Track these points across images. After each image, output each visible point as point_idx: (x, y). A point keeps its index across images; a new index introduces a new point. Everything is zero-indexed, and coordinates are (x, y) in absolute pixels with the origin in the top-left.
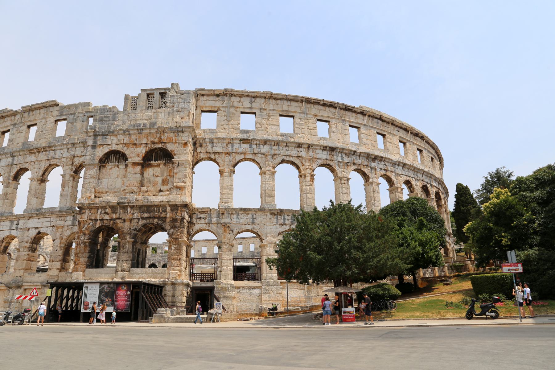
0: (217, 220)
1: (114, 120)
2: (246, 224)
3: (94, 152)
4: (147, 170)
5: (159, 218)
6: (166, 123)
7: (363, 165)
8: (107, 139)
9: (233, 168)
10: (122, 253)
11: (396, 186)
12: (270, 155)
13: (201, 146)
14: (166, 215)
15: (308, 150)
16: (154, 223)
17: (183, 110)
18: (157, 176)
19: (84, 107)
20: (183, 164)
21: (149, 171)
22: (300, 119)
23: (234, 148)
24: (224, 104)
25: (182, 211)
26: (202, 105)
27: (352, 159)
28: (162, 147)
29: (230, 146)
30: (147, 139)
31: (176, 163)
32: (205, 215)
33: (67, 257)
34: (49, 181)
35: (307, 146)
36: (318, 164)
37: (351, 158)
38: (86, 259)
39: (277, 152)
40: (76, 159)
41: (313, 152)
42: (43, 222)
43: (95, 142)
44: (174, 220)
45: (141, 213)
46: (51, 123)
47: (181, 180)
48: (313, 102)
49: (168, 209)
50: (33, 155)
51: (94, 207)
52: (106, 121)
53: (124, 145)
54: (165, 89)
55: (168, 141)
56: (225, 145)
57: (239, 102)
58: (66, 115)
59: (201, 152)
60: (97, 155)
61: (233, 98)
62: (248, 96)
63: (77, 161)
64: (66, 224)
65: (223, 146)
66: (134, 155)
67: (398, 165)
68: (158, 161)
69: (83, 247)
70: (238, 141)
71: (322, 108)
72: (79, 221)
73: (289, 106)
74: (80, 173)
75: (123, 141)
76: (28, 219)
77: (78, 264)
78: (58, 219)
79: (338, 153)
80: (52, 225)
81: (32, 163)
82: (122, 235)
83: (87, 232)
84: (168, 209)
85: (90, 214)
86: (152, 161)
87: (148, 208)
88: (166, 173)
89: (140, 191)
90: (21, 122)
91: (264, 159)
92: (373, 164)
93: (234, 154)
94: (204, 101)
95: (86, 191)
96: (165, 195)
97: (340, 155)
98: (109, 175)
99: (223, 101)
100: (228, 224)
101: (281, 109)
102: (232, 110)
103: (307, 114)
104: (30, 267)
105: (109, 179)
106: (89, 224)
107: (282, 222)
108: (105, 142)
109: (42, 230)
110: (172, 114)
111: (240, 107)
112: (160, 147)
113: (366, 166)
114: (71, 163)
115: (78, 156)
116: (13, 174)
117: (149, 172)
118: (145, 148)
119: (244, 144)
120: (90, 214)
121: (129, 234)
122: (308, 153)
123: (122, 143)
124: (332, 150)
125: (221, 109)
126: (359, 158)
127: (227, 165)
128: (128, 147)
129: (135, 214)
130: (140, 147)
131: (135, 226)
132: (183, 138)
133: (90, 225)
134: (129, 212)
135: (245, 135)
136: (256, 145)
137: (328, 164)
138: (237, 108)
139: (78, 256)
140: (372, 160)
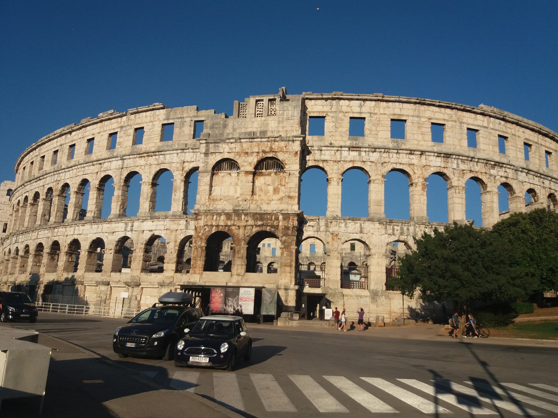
0: (325, 228)
1: (225, 126)
2: (354, 233)
3: (207, 160)
4: (259, 178)
5: (272, 226)
6: (277, 131)
7: (481, 173)
8: (218, 147)
9: (341, 177)
10: (238, 258)
11: (517, 195)
12: (380, 163)
14: (279, 223)
15: (421, 157)
16: (268, 230)
17: (293, 118)
18: (269, 185)
19: (191, 111)
20: (294, 173)
21: (260, 179)
22: (413, 123)
23: (343, 155)
24: (333, 110)
25: (294, 220)
27: (469, 166)
28: (273, 156)
29: (338, 153)
30: (259, 148)
31: (287, 173)
32: (313, 223)
33: (181, 259)
34: (158, 185)
35: (419, 153)
36: (431, 171)
37: (468, 165)
38: (203, 263)
39: (387, 160)
40: (186, 164)
41: (426, 159)
42: (157, 226)
43: (207, 150)
44: (287, 228)
45: (255, 220)
46: (159, 127)
47: (293, 189)
48: (428, 103)
49: (281, 217)
50: (143, 158)
51: (209, 213)
52: (217, 128)
53: (236, 154)
55: (279, 150)
57: (348, 106)
58: (173, 119)
60: (210, 163)
61: (342, 102)
63: (188, 167)
64: (180, 228)
65: (332, 154)
66: (246, 164)
67: (521, 171)
69: (200, 251)
70: (347, 149)
71: (437, 109)
72: (195, 226)
73: (401, 109)
74: (189, 178)
75: (235, 149)
76: (143, 222)
77: (196, 267)
78: (172, 222)
79: (453, 159)
80: (166, 228)
81: (143, 167)
82: (236, 241)
83: (203, 238)
84: (281, 217)
85: (206, 220)
86: (263, 169)
87: (260, 216)
88: (277, 182)
90: (128, 125)
91: (373, 167)
92: (493, 172)
93: (342, 162)
94: (312, 106)
95: (201, 198)
96: (278, 204)
97: (456, 162)
98: (222, 182)
99: (332, 106)
100: (336, 233)
101: (392, 113)
102: (341, 115)
103: (421, 117)
105: (222, 187)
106: (205, 229)
107: (391, 232)
108: (217, 150)
109: (156, 233)
110: (283, 122)
111: (348, 112)
113: (484, 174)
114: (182, 168)
115: (188, 162)
117: (260, 181)
118: (257, 157)
119: (353, 152)
120: (206, 220)
121: (243, 240)
122: (420, 160)
124: (447, 156)
125: (329, 114)
126: (477, 165)
127: (336, 173)
129: (249, 221)
130: (252, 156)
131: (249, 233)
132: (294, 148)
133: (206, 231)
134: (242, 219)
135: (354, 142)
136: (365, 151)
137: (441, 171)
138: (346, 113)
139: (196, 260)
140: (492, 167)
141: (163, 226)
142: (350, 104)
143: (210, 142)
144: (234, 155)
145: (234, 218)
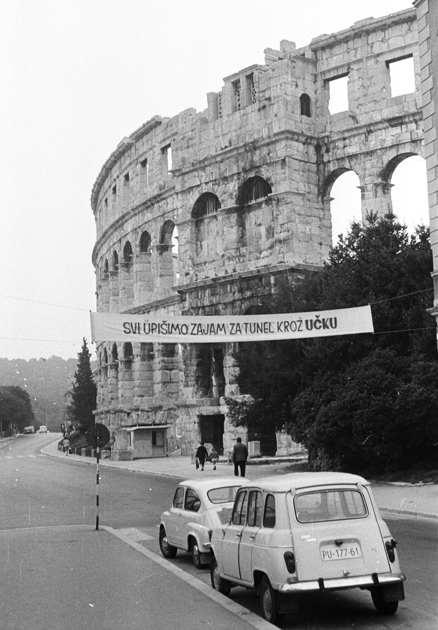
9: (380, 180)
13: (328, 151)
14: (271, 290)
26: (322, 70)
29: (372, 137)
30: (238, 166)
50: (149, 209)
53: (214, 183)
54: (251, 68)
56: (363, 137)
57: (382, 41)
59: (329, 162)
61: (372, 38)
62: (396, 23)
66: (225, 197)
68: (258, 198)
76: (156, 310)
89: (240, 254)
93: (378, 151)
104: (169, 378)
111: (382, 54)
112: (254, 175)
116: (138, 243)
118: (237, 181)
119: (395, 128)
123: (211, 179)
125: (352, 67)
127: (370, 175)
128: (219, 185)
138: (378, 55)
141: (173, 313)
142: (385, 36)
143: (184, 171)
144: (212, 185)
145: (220, 291)
